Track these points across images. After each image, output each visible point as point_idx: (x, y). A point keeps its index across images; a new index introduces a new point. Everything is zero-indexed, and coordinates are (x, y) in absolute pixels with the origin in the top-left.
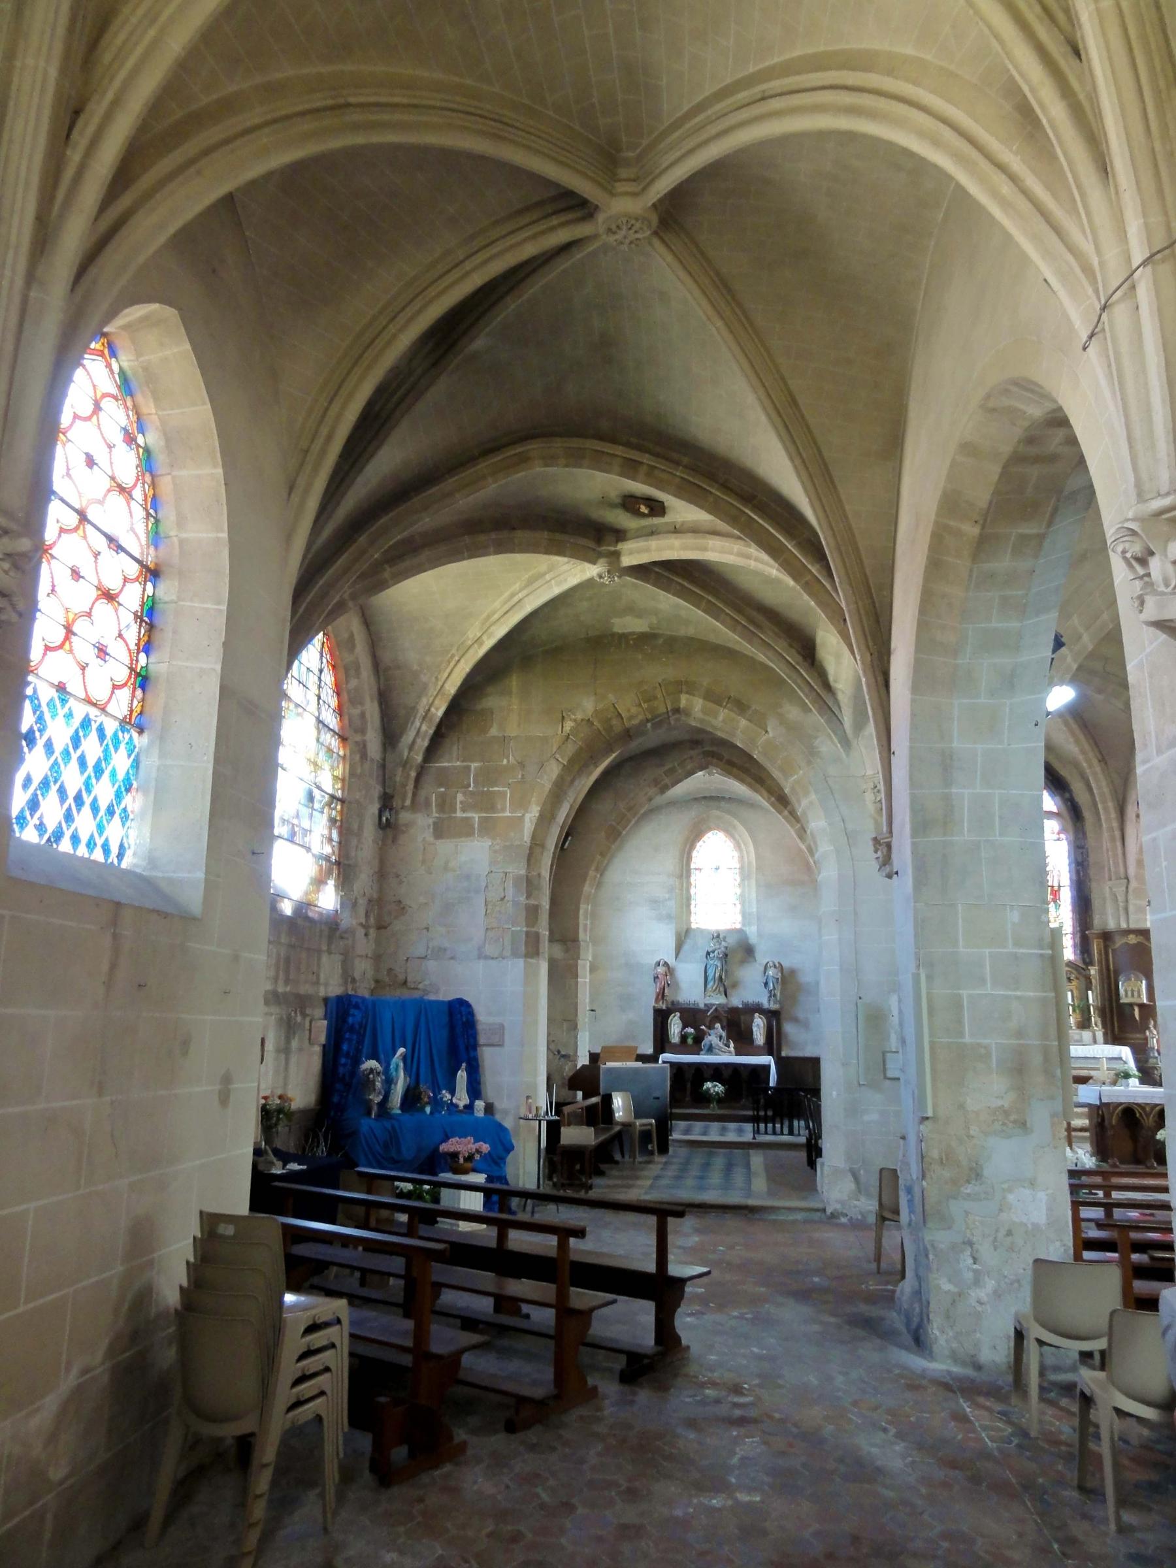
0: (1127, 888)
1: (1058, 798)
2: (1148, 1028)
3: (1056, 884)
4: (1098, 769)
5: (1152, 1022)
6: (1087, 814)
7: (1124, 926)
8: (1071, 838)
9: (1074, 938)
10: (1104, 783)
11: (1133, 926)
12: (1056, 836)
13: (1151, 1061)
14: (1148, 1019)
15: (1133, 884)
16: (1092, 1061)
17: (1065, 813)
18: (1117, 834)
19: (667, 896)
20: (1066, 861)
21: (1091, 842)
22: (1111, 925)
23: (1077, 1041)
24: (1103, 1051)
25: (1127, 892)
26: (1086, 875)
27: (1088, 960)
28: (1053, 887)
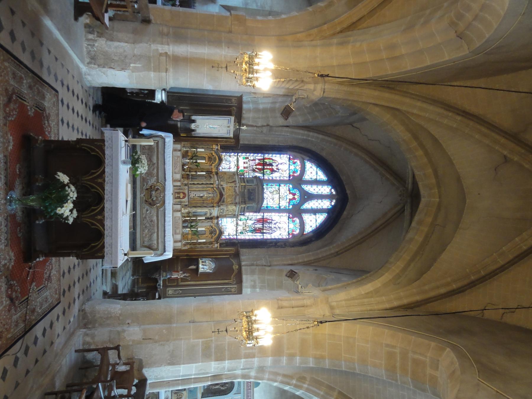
0: (265, 266)
1: (311, 234)
2: (184, 273)
3: (264, 231)
4: (333, 251)
5: (187, 275)
6: (304, 248)
7: (243, 263)
8: (290, 240)
9: (234, 239)
10: (324, 255)
11: (243, 268)
12: (290, 232)
13: (164, 274)
14: (189, 273)
15: (268, 268)
16: (163, 235)
17: (304, 237)
18: (296, 262)
19: (259, 4)
20: (277, 237)
21: (289, 249)
22: (242, 258)
23: (175, 231)
24: (170, 241)
25: (262, 266)
26: (271, 246)
27: (223, 246)
28: (263, 229)
